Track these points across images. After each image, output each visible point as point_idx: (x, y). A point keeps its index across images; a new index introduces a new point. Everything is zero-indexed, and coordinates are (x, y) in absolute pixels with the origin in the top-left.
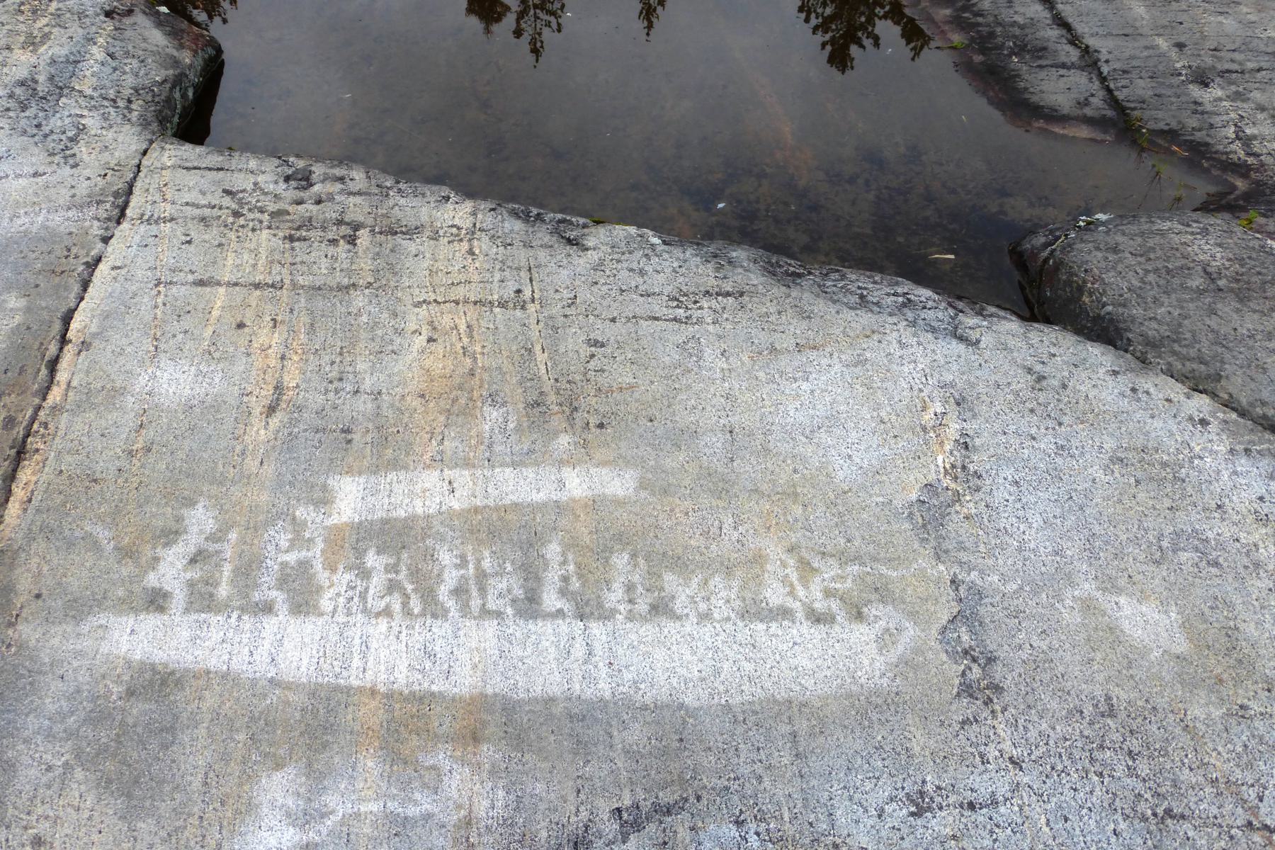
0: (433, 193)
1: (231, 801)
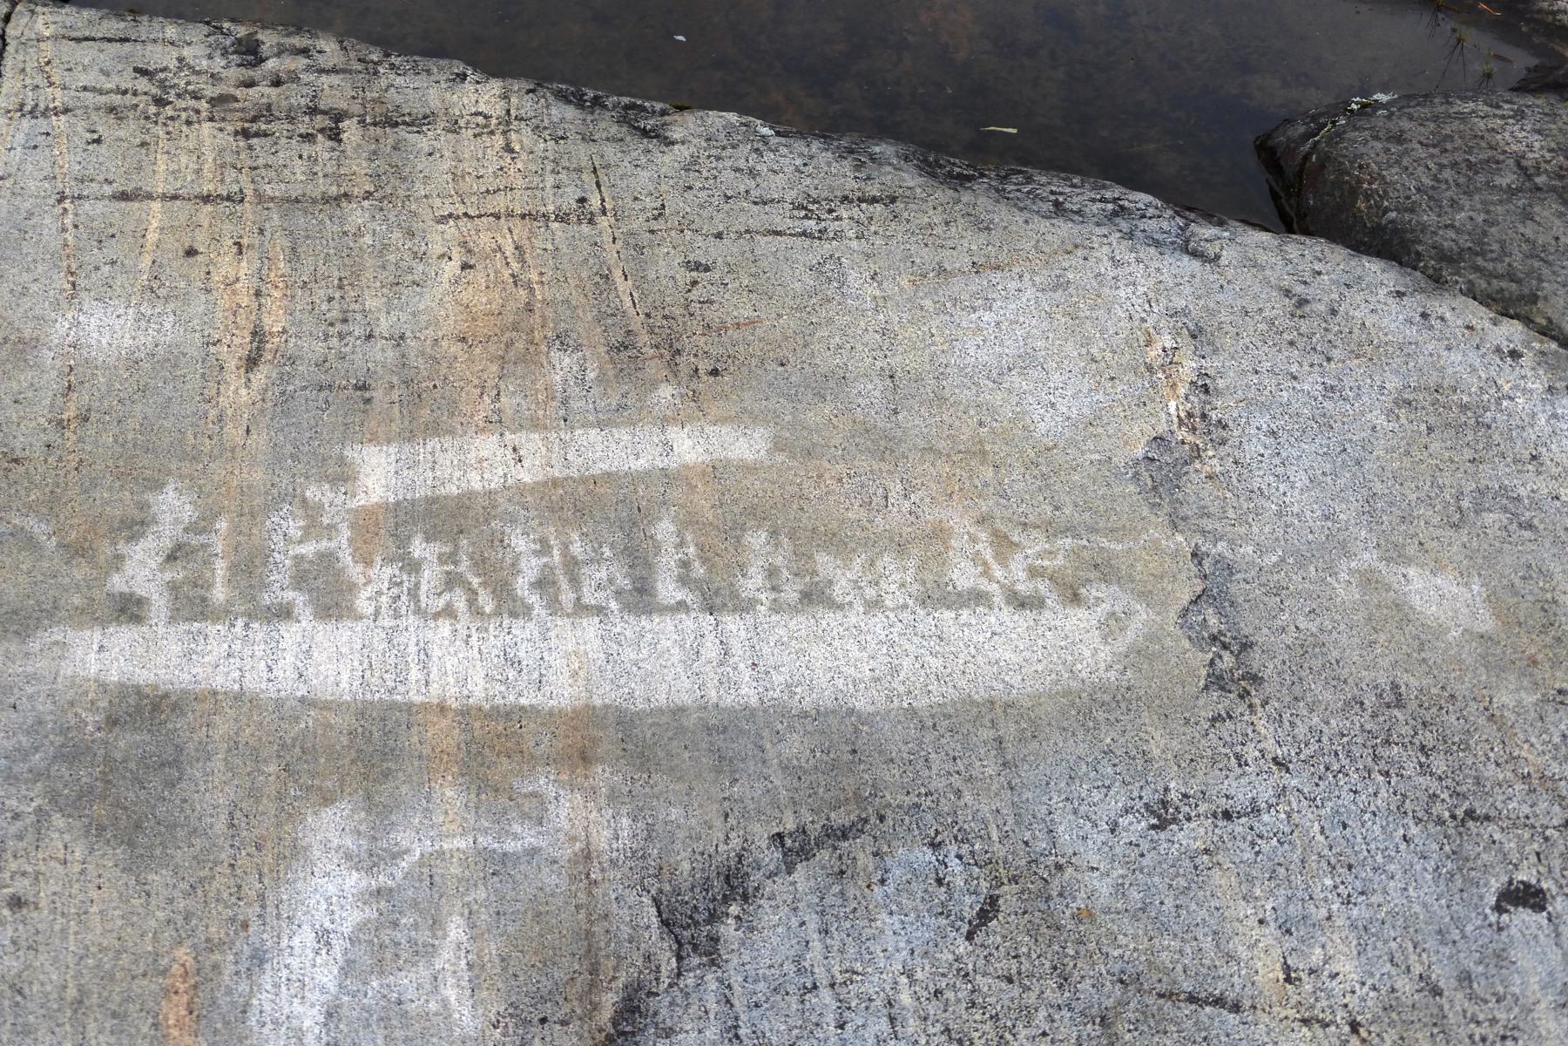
0: (441, 69)
1: (269, 845)
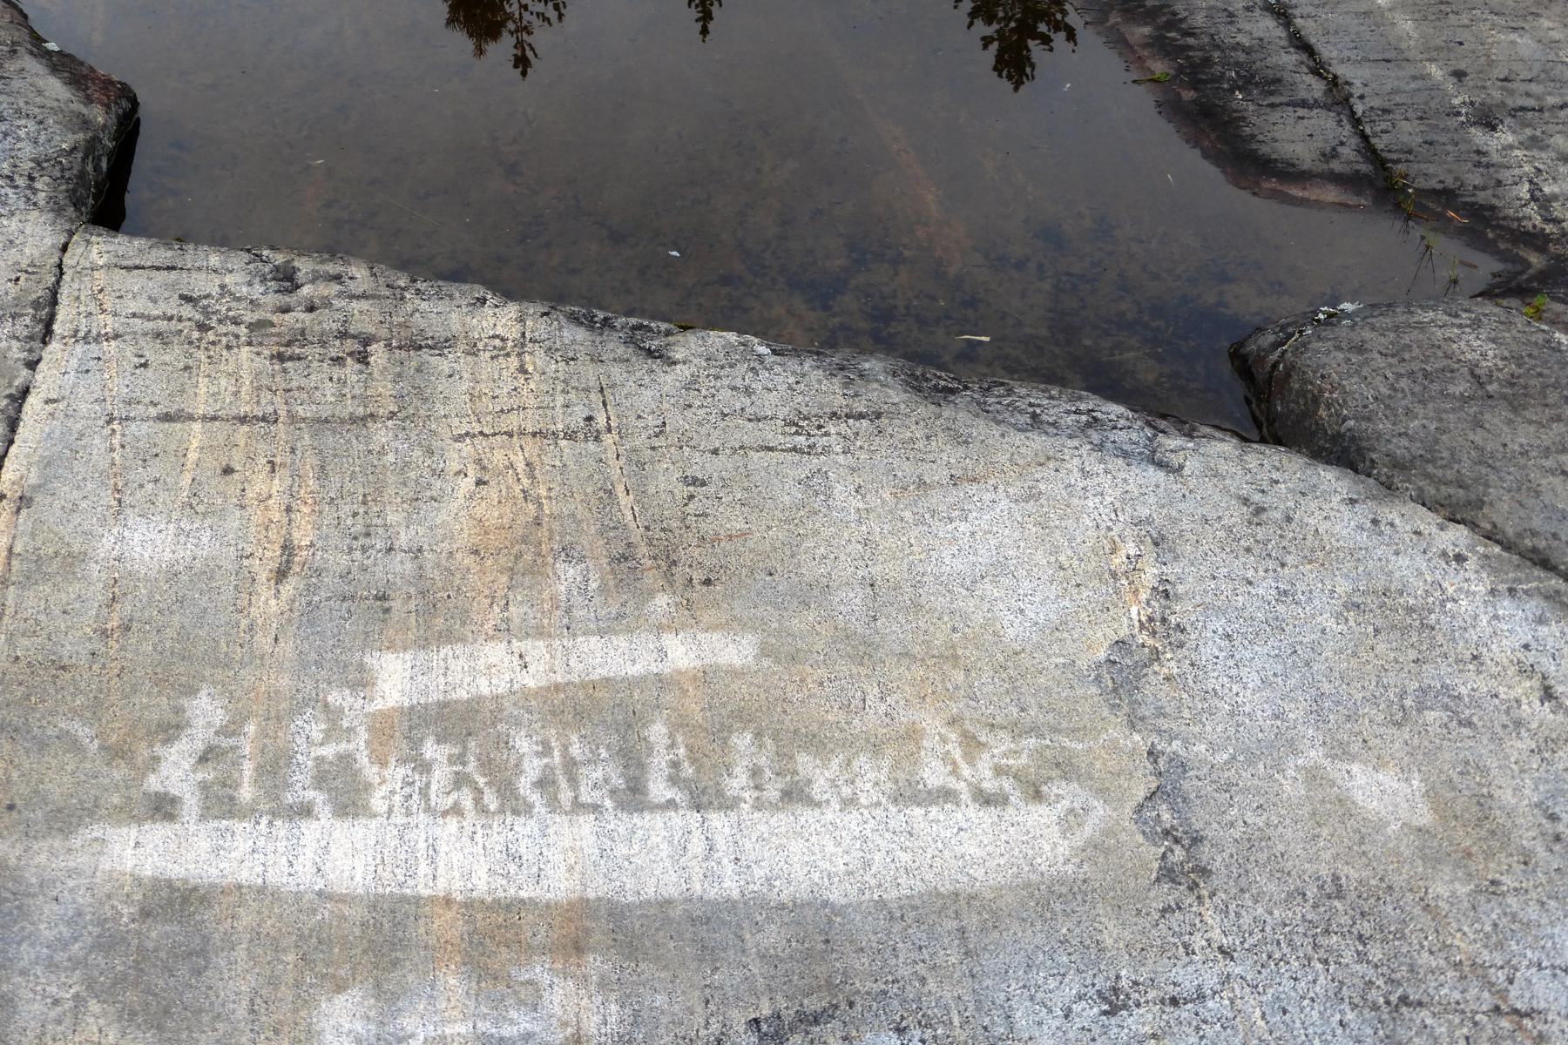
0: (463, 294)
1: (286, 1029)
